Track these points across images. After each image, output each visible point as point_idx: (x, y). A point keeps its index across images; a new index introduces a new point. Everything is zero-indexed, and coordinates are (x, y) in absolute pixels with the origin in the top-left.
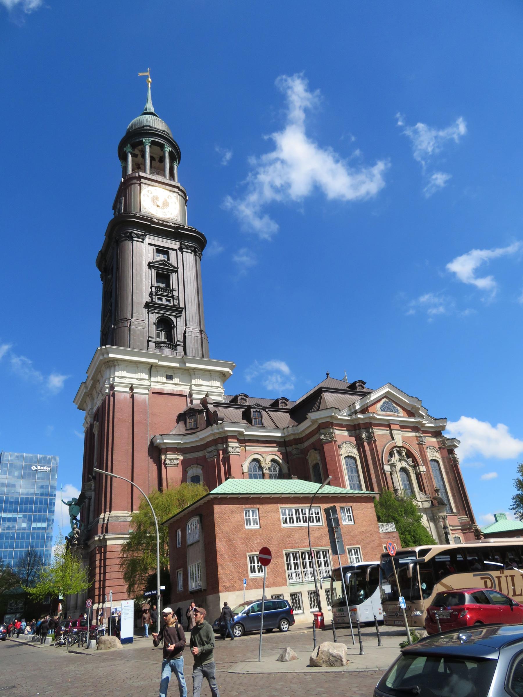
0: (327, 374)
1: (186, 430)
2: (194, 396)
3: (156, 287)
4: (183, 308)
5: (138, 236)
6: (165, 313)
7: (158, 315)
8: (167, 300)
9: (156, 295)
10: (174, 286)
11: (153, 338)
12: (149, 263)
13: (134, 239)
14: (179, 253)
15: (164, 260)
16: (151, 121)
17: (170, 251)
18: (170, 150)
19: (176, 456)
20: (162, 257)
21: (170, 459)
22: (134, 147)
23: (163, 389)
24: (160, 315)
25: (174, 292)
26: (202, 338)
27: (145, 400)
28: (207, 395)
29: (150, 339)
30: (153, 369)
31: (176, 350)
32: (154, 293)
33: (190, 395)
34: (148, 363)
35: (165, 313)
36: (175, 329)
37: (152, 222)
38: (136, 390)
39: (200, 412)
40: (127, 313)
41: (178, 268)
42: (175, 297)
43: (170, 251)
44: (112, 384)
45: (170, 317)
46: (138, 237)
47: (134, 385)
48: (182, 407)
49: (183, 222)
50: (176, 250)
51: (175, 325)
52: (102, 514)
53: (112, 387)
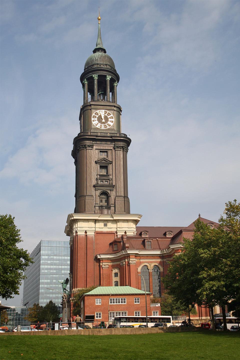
0: (199, 215)
1: (113, 251)
2: (118, 234)
3: (99, 175)
4: (114, 185)
5: (89, 146)
6: (104, 189)
8: (105, 181)
9: (100, 179)
10: (110, 172)
11: (98, 204)
12: (96, 161)
13: (87, 148)
14: (113, 150)
15: (104, 158)
16: (98, 59)
17: (108, 151)
18: (110, 78)
19: (107, 264)
20: (104, 155)
21: (104, 265)
22: (88, 80)
23: (102, 231)
24: (101, 191)
25: (110, 176)
26: (125, 201)
27: (93, 237)
28: (125, 233)
29: (96, 205)
30: (97, 221)
31: (110, 209)
32: (98, 179)
33: (117, 233)
34: (94, 219)
35: (104, 189)
36: (110, 197)
37: (97, 136)
38: (88, 233)
39: (120, 242)
40: (84, 193)
41: (112, 162)
42: (110, 179)
43: (108, 151)
44: (76, 231)
45: (107, 191)
46: (89, 147)
47: (87, 231)
48: (111, 239)
49: (117, 129)
50: (112, 150)
51: (110, 195)
52: (74, 289)
53: (76, 232)
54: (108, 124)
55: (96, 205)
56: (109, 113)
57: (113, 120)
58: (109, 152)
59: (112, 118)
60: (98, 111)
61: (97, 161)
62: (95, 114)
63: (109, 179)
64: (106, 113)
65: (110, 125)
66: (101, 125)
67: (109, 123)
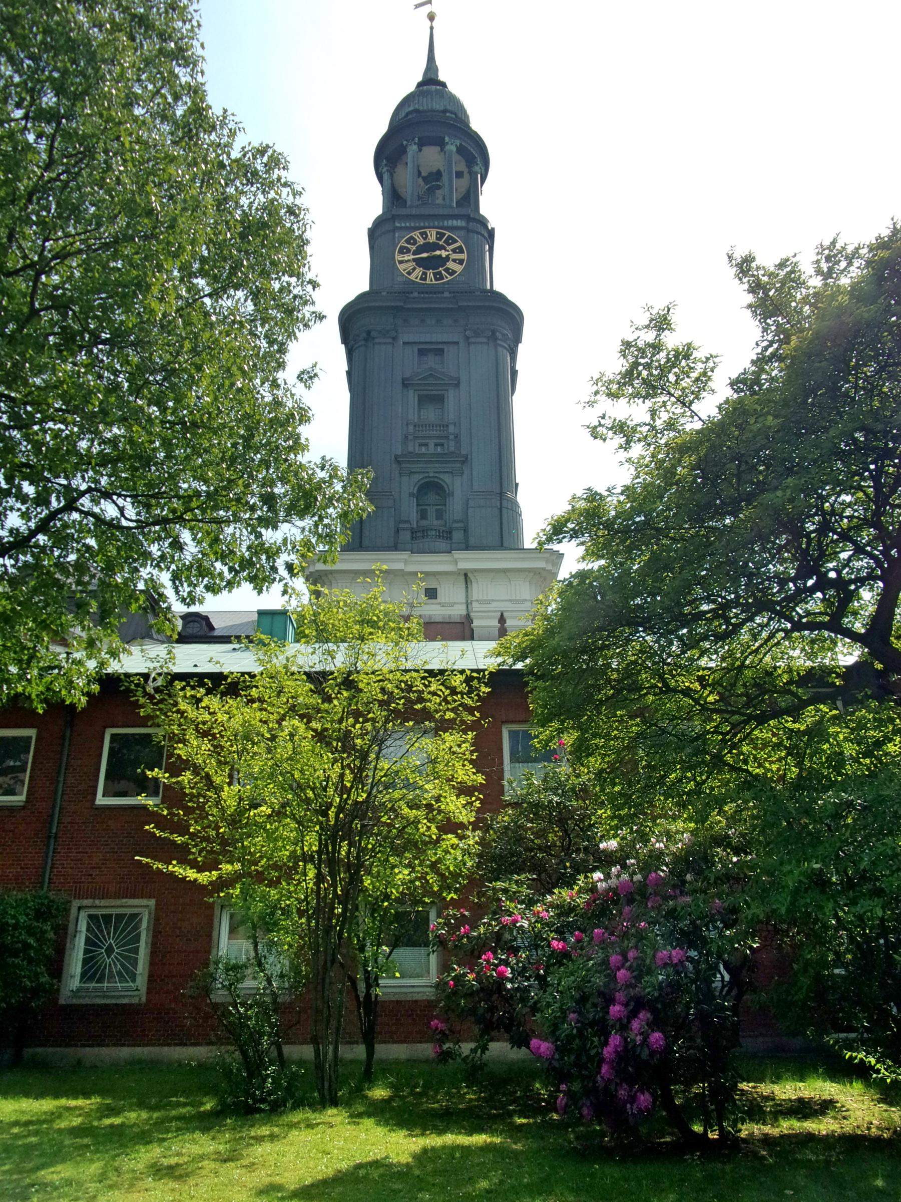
2: (476, 623)
7: (417, 477)
8: (436, 445)
9: (416, 438)
12: (403, 380)
29: (401, 526)
32: (410, 437)
45: (441, 476)
50: (457, 343)
54: (447, 270)
55: (401, 526)
56: (449, 237)
57: (464, 256)
58: (450, 352)
59: (462, 252)
60: (416, 235)
61: (407, 379)
62: (407, 241)
63: (447, 438)
64: (440, 236)
65: (454, 272)
66: (425, 274)
67: (451, 265)
